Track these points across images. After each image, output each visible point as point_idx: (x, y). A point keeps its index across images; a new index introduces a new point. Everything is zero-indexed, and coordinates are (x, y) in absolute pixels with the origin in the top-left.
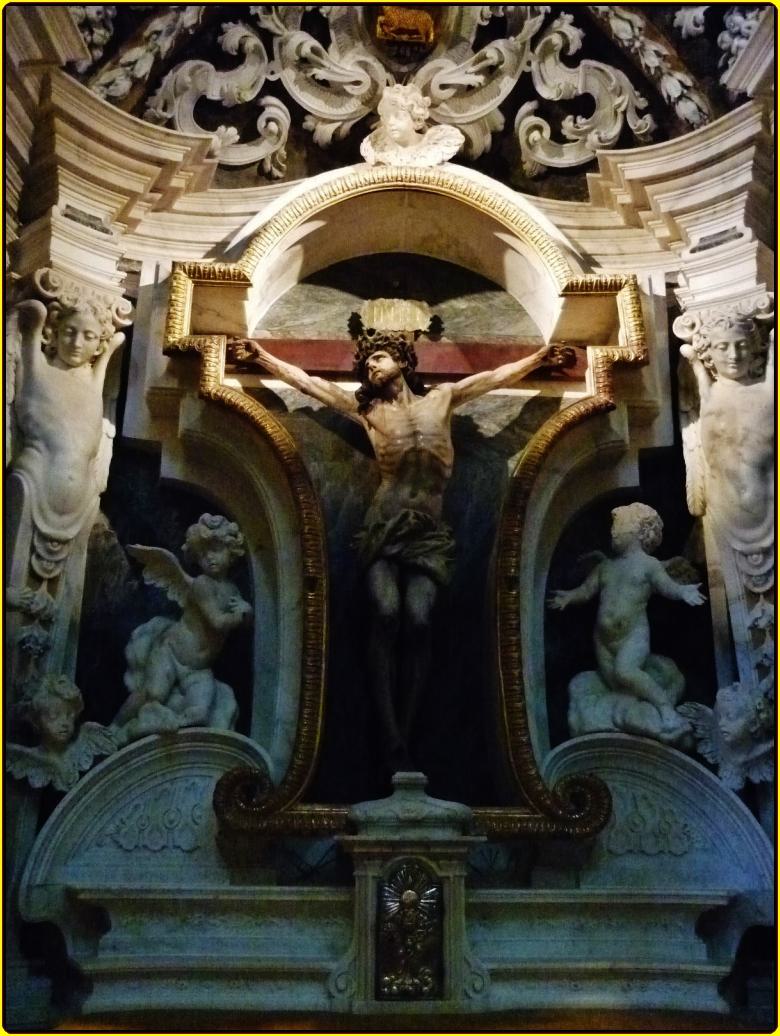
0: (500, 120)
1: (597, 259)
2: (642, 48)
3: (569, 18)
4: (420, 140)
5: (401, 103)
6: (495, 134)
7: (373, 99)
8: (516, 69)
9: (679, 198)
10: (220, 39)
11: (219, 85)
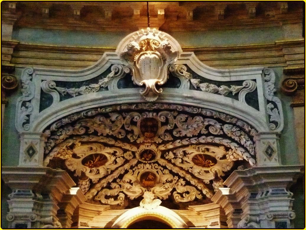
0: (170, 194)
1: (197, 215)
2: (197, 185)
3: (182, 179)
4: (152, 202)
5: (148, 195)
6: (169, 196)
7: (143, 193)
8: (172, 187)
9: (206, 215)
10: (110, 185)
11: (109, 192)
